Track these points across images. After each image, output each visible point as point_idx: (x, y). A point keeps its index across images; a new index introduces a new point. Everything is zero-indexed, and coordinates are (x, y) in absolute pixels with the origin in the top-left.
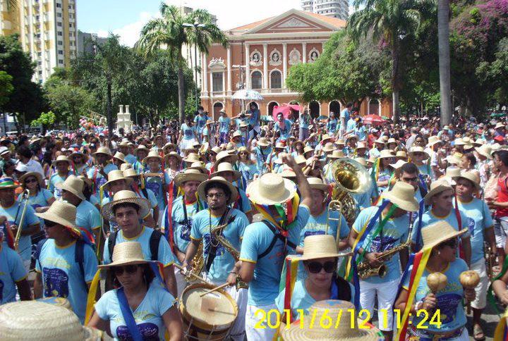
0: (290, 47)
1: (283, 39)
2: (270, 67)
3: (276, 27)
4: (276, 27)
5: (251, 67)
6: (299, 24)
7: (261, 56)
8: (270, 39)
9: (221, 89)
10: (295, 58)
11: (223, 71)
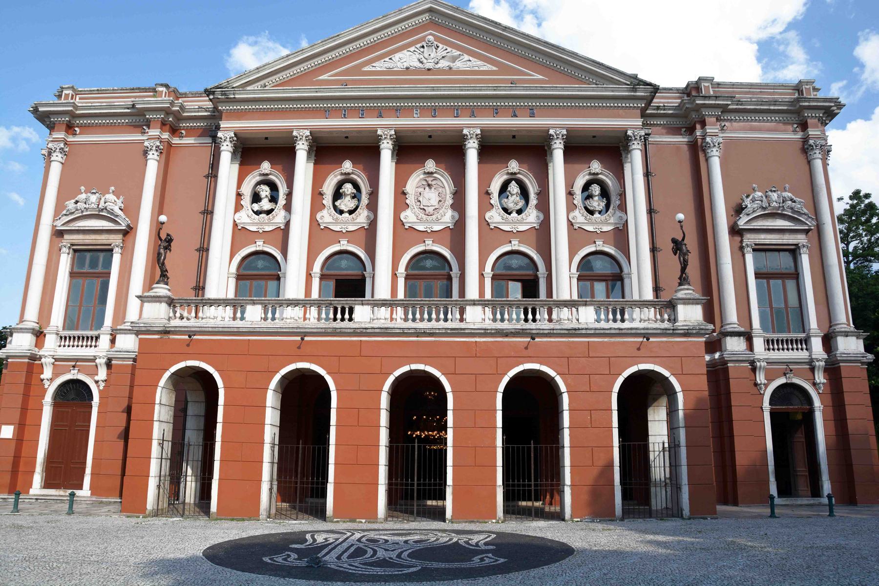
0: (410, 150)
1: (380, 114)
2: (318, 234)
3: (357, 70)
4: (357, 70)
6: (454, 59)
7: (282, 190)
8: (326, 113)
9: (100, 324)
10: (431, 197)
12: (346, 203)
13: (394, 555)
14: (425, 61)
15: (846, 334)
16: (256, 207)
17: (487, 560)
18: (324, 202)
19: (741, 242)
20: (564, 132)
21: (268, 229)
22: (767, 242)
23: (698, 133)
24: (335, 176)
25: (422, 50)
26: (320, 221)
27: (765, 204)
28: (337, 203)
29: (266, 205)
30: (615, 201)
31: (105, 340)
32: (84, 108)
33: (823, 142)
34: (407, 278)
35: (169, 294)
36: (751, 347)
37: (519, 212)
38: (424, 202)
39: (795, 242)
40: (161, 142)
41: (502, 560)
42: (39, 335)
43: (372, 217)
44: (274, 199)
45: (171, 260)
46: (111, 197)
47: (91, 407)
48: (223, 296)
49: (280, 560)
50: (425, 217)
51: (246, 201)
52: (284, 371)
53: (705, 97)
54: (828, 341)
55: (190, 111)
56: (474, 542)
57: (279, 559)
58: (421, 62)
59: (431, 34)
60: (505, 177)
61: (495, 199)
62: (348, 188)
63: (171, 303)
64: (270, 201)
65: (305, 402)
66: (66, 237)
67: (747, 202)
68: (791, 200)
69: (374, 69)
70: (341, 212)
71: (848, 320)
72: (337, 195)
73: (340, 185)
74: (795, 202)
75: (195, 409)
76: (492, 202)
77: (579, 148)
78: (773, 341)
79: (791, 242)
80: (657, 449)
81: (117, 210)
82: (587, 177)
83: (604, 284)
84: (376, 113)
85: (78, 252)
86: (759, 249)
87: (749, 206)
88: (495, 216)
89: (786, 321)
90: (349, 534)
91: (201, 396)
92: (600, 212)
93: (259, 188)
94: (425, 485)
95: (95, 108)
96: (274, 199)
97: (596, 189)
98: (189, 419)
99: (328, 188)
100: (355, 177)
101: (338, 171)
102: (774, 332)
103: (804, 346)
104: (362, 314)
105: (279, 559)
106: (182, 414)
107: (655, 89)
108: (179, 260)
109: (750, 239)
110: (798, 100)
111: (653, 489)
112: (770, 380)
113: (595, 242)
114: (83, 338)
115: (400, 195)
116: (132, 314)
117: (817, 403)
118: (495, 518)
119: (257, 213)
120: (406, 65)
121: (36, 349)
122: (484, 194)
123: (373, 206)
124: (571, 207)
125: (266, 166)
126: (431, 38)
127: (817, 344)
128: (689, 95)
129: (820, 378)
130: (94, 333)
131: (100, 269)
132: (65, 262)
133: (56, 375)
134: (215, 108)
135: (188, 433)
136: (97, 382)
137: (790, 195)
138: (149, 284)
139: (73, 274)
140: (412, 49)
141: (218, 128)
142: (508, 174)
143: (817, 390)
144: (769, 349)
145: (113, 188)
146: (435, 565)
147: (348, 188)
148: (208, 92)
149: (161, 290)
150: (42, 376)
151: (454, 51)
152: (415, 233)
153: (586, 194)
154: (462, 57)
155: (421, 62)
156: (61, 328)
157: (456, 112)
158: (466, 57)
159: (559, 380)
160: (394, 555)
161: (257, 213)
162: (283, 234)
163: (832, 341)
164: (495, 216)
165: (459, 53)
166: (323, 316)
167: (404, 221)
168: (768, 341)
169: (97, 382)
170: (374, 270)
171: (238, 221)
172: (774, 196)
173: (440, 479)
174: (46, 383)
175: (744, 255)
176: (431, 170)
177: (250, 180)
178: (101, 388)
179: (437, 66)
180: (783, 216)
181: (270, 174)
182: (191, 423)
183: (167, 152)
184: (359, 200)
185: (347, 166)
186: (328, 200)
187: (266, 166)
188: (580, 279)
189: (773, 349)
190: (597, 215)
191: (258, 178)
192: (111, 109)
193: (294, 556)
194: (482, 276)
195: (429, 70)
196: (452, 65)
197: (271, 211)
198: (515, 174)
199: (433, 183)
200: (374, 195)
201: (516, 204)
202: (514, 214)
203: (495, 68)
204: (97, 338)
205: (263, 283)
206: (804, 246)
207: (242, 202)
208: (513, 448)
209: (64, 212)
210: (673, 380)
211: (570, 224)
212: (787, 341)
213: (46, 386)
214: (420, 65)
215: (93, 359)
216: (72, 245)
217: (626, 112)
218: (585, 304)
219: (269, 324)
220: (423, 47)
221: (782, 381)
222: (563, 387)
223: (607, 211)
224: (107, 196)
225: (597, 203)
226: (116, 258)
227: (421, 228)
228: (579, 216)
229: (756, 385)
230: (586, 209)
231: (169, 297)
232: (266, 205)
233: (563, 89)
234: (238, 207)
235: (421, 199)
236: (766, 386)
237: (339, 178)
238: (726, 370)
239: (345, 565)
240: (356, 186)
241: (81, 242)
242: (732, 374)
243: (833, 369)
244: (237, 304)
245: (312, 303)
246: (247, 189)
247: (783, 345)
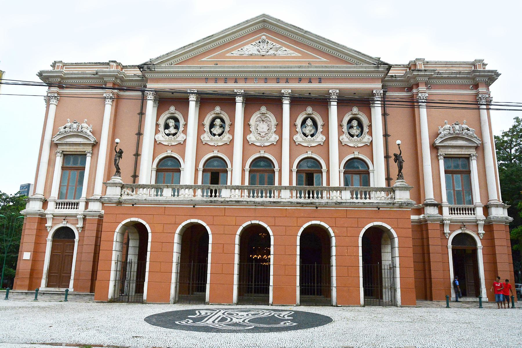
0: (253, 101)
3: (222, 55)
5: (157, 144)
7: (182, 122)
10: (263, 127)
11: (89, 149)
12: (217, 130)
13: (241, 321)
14: (261, 51)
15: (497, 206)
16: (167, 131)
17: (288, 324)
18: (205, 129)
19: (437, 152)
20: (338, 91)
21: (173, 144)
22: (452, 153)
23: (415, 91)
24: (211, 115)
25: (259, 44)
26: (203, 140)
27: (452, 132)
28: (212, 130)
29: (172, 130)
30: (366, 130)
31: (82, 205)
32: (68, 74)
33: (487, 96)
34: (250, 172)
35: (121, 182)
36: (441, 212)
37: (312, 135)
38: (260, 130)
39: (469, 153)
40: (113, 94)
41: (295, 324)
42: (45, 203)
43: (231, 138)
44: (177, 127)
45: (122, 163)
46: (85, 125)
47: (74, 242)
48: (149, 183)
49: (184, 323)
50: (260, 138)
51: (161, 128)
52: (184, 224)
53: (419, 70)
54: (486, 209)
55: (128, 76)
56: (282, 316)
57: (184, 323)
58: (259, 51)
59: (264, 35)
60: (305, 116)
61: (299, 129)
62: (218, 122)
63: (122, 187)
64: (175, 128)
65: (195, 241)
66: (59, 147)
67: (441, 130)
68: (468, 129)
69: (232, 55)
70: (214, 135)
71: (498, 197)
72: (212, 125)
73: (213, 120)
74: (469, 130)
75: (133, 244)
76: (297, 130)
77: (345, 101)
78: (454, 209)
79: (466, 153)
80: (386, 268)
81: (88, 132)
82: (351, 116)
83: (358, 176)
84: (234, 81)
85: (65, 156)
86: (447, 158)
87: (442, 132)
88: (299, 138)
89: (462, 198)
90: (218, 311)
91: (137, 236)
92: (357, 136)
93: (168, 121)
94: (258, 285)
95: (75, 74)
96: (177, 127)
97: (355, 123)
98: (130, 248)
99: (207, 122)
100: (222, 115)
101: (213, 112)
102: (455, 204)
103: (472, 212)
104: (225, 194)
105: (184, 323)
106: (126, 246)
107: (389, 67)
108: (126, 163)
109: (442, 152)
110: (474, 71)
111: (384, 290)
112: (452, 231)
113: (354, 153)
114: (70, 204)
115: (247, 125)
116: (98, 191)
117: (479, 244)
118: (295, 304)
119: (168, 135)
120: (250, 53)
121: (43, 210)
122: (293, 125)
123: (232, 132)
124: (340, 133)
125: (172, 109)
126: (264, 37)
127: (479, 212)
128: (410, 68)
129: (481, 231)
130: (76, 201)
131: (79, 165)
132: (59, 161)
133: (54, 224)
134: (144, 76)
135: (130, 257)
136: (77, 228)
137: (466, 126)
138: (108, 176)
139: (63, 168)
140: (253, 43)
141: (145, 86)
142: (306, 114)
143: (479, 237)
144: (452, 214)
145: (86, 120)
146: (262, 325)
147: (218, 122)
148: (140, 67)
149: (117, 180)
150: (46, 225)
151: (277, 45)
152: (255, 147)
153: (349, 125)
154: (281, 48)
155: (259, 51)
156: (57, 199)
157: (278, 80)
158: (284, 48)
159: (330, 230)
160: (241, 321)
161: (168, 135)
162: (182, 145)
163: (489, 209)
164: (299, 138)
165: (280, 46)
166: (205, 194)
167: (249, 140)
168: (451, 209)
169: (77, 228)
170: (232, 167)
171: (157, 139)
172: (457, 127)
173: (267, 282)
174: (49, 229)
175: (438, 160)
176: (264, 112)
177: (164, 117)
178: (80, 231)
179: (268, 54)
181: (175, 113)
182: (131, 251)
183: (117, 100)
184: (224, 128)
185: (218, 109)
186: (207, 128)
187: (172, 109)
188: (345, 173)
189: (455, 214)
190: (355, 137)
191: (169, 115)
192: (84, 75)
193: (191, 321)
194: (291, 171)
195: (263, 56)
196: (276, 53)
197: (176, 133)
198: (310, 114)
199: (264, 119)
200: (232, 125)
201: (311, 131)
202: (309, 137)
203: (300, 55)
204: (78, 204)
205: (171, 173)
207: (159, 129)
208: (305, 266)
209: (58, 133)
210: (392, 231)
211: (340, 142)
213: (48, 231)
214: (259, 53)
215: (75, 216)
216: (63, 151)
217: (372, 80)
218: (345, 189)
219: (176, 198)
220: (260, 42)
221: (459, 231)
222: (332, 234)
223: (361, 135)
224: (83, 124)
225: (355, 131)
226: (88, 159)
227: (258, 144)
228: (345, 138)
229: (444, 233)
230: (349, 133)
231: (121, 184)
232: (172, 130)
233: (337, 67)
234: (157, 132)
235: (258, 128)
236: (450, 234)
237: (214, 116)
238: (426, 225)
239: (217, 325)
240: (222, 120)
241: (68, 150)
242: (430, 227)
243: (489, 226)
244: (158, 188)
245: (199, 187)
246: (162, 122)
247: (460, 211)
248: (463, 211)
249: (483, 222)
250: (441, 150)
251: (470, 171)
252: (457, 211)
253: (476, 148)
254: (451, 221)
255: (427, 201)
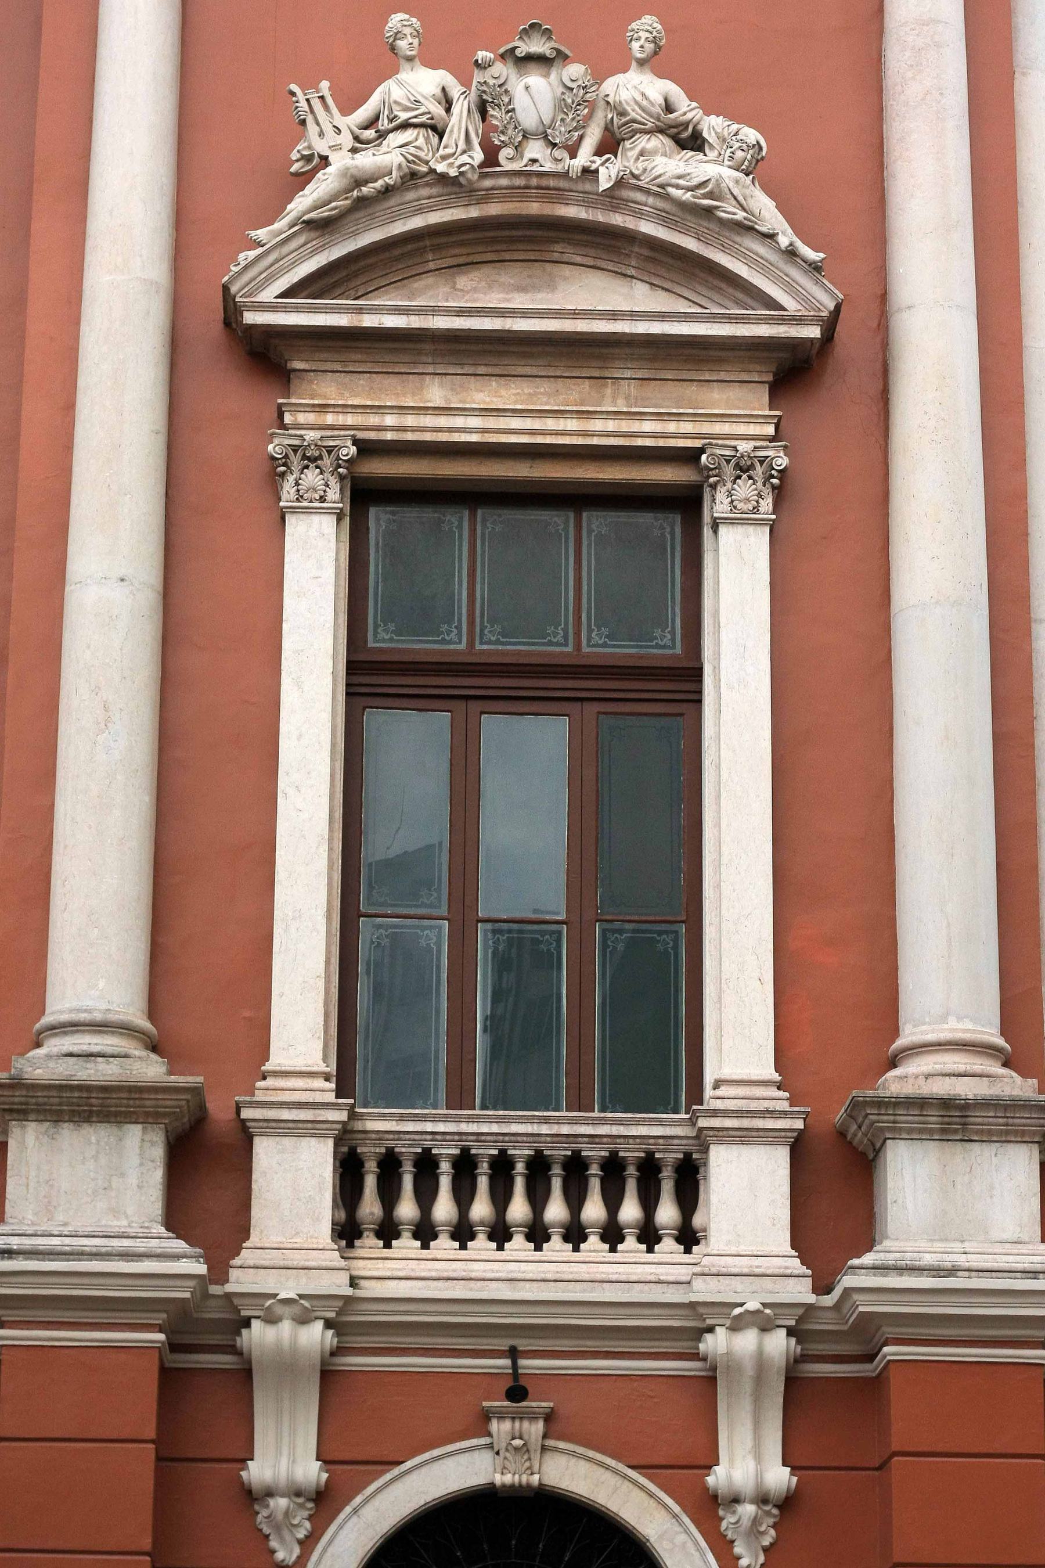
22: (468, 429)
27: (458, 154)
39: (680, 433)
79: (647, 431)
103: (667, 1213)
109: (338, 407)
129: (750, 1460)
172: (534, 96)
180: (607, 246)
206: (743, 469)
212: (538, 1167)
236: (324, 1503)
248: (537, 1199)
249: (779, 1344)
250: (329, 389)
251: (696, 674)
252: (463, 1197)
253: (793, 370)
254: (345, 1318)
255: (55, 1045)
